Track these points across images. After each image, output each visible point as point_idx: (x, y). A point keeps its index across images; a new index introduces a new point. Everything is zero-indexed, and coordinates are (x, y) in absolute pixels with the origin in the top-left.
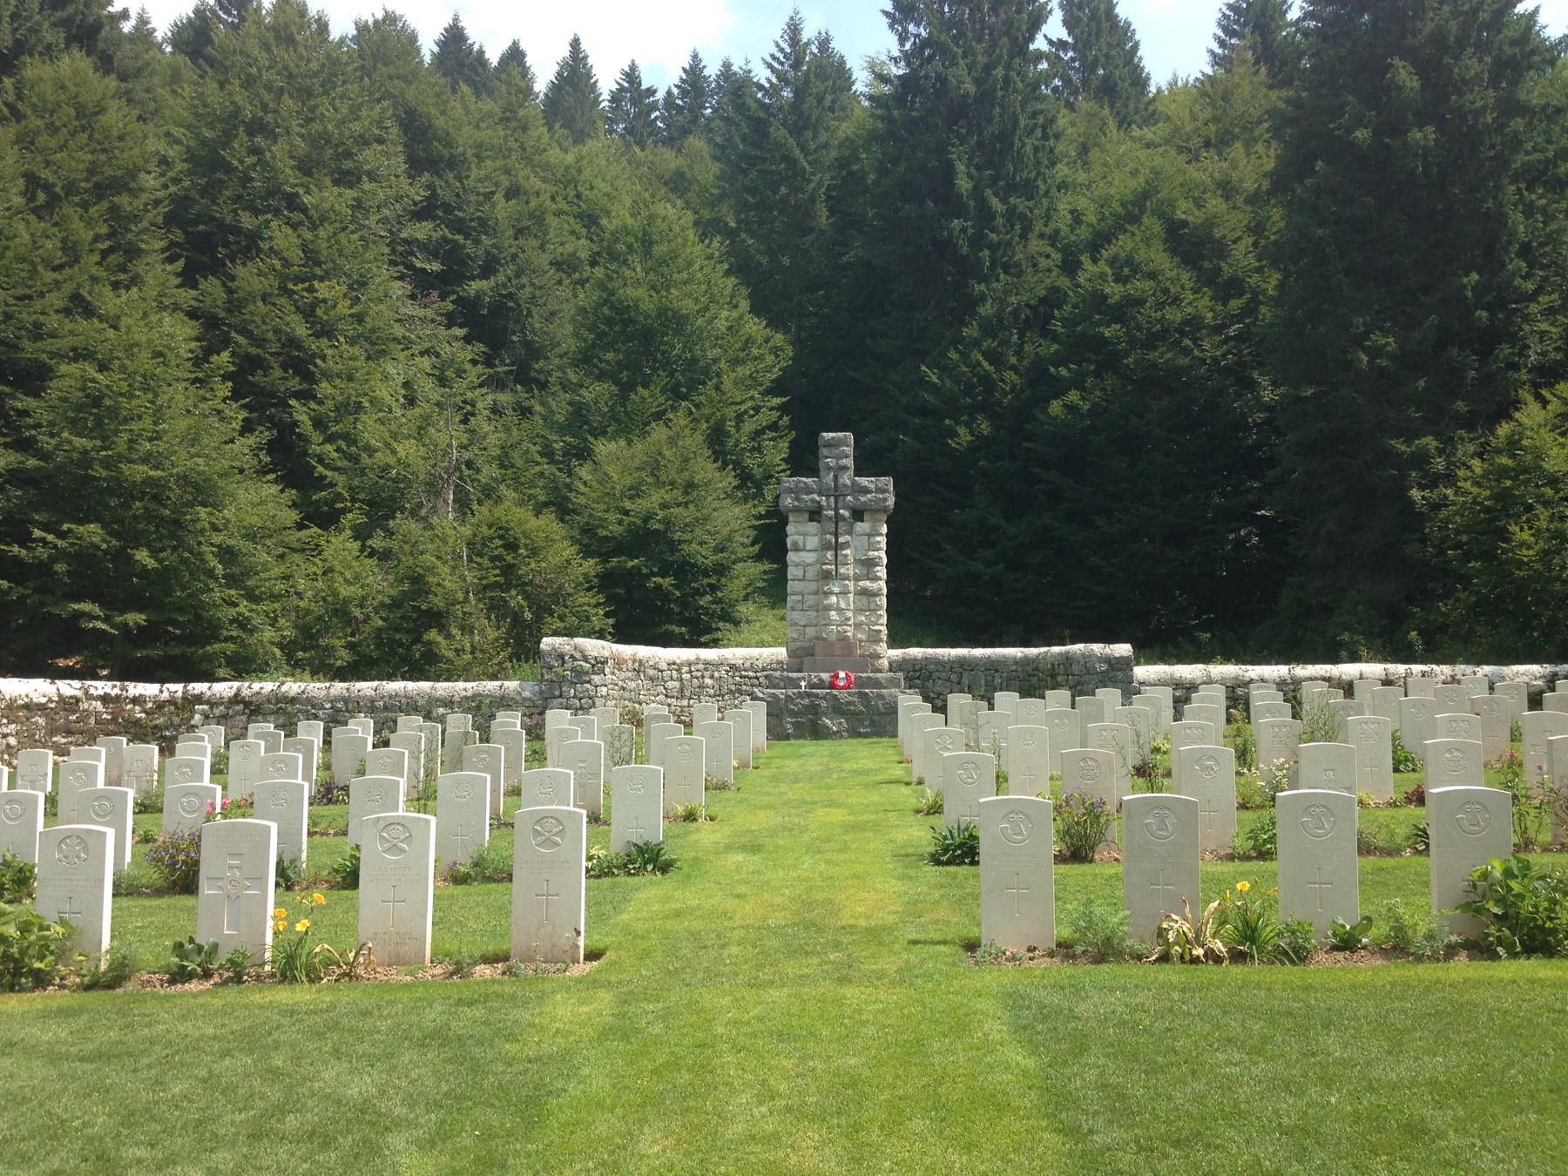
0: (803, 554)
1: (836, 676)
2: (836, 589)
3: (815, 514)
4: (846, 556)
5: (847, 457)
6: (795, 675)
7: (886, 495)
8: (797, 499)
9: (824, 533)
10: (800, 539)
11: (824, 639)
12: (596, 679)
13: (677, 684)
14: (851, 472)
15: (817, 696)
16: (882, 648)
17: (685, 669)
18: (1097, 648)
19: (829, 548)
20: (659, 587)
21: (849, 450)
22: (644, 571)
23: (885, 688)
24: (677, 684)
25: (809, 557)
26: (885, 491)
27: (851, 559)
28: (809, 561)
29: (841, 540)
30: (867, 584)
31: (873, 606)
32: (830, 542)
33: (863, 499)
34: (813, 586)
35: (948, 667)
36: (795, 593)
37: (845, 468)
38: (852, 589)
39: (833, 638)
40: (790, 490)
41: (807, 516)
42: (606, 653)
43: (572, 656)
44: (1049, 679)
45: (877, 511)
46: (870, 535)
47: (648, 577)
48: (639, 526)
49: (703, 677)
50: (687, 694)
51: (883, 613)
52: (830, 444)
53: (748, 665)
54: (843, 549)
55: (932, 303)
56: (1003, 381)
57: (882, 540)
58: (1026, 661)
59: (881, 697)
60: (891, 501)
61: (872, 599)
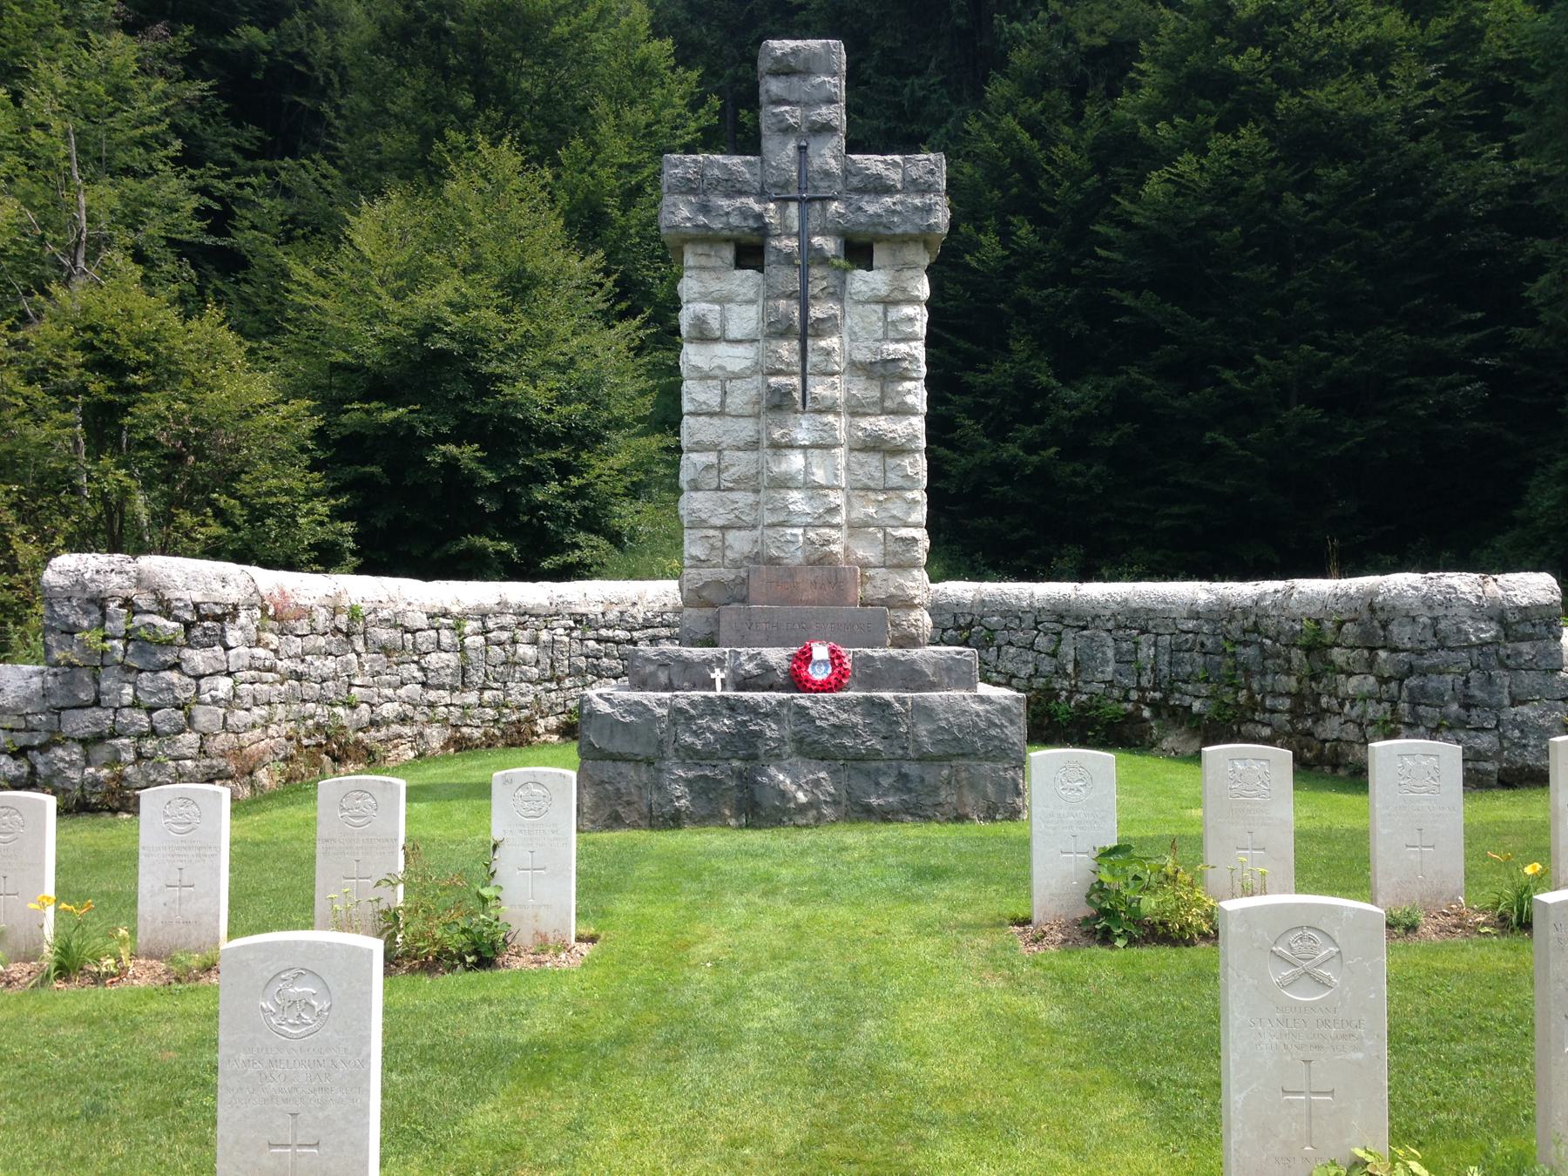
0: (721, 349)
1: (805, 657)
2: (802, 435)
3: (750, 253)
4: (828, 353)
5: (831, 101)
6: (697, 653)
7: (930, 198)
8: (705, 209)
9: (771, 294)
10: (711, 311)
11: (773, 561)
12: (198, 659)
13: (452, 659)
14: (839, 141)
15: (753, 709)
16: (919, 584)
17: (471, 626)
18: (1463, 583)
19: (783, 334)
20: (451, 464)
21: (836, 84)
22: (422, 430)
23: (933, 686)
24: (452, 659)
25: (736, 358)
26: (925, 189)
27: (838, 362)
28: (735, 366)
29: (816, 312)
30: (882, 424)
31: (894, 479)
32: (787, 317)
33: (872, 208)
34: (746, 429)
35: (1029, 620)
36: (700, 447)
37: (826, 129)
38: (841, 435)
39: (794, 556)
40: (687, 187)
41: (728, 253)
42: (233, 595)
43: (127, 603)
44: (1297, 655)
45: (905, 240)
46: (888, 302)
47: (429, 443)
48: (409, 347)
49: (514, 642)
50: (477, 677)
51: (920, 496)
52: (785, 69)
53: (613, 615)
54: (819, 335)
55: (932, 65)
56: (1050, 161)
57: (919, 318)
58: (1222, 614)
59: (925, 711)
60: (941, 217)
61: (892, 462)
